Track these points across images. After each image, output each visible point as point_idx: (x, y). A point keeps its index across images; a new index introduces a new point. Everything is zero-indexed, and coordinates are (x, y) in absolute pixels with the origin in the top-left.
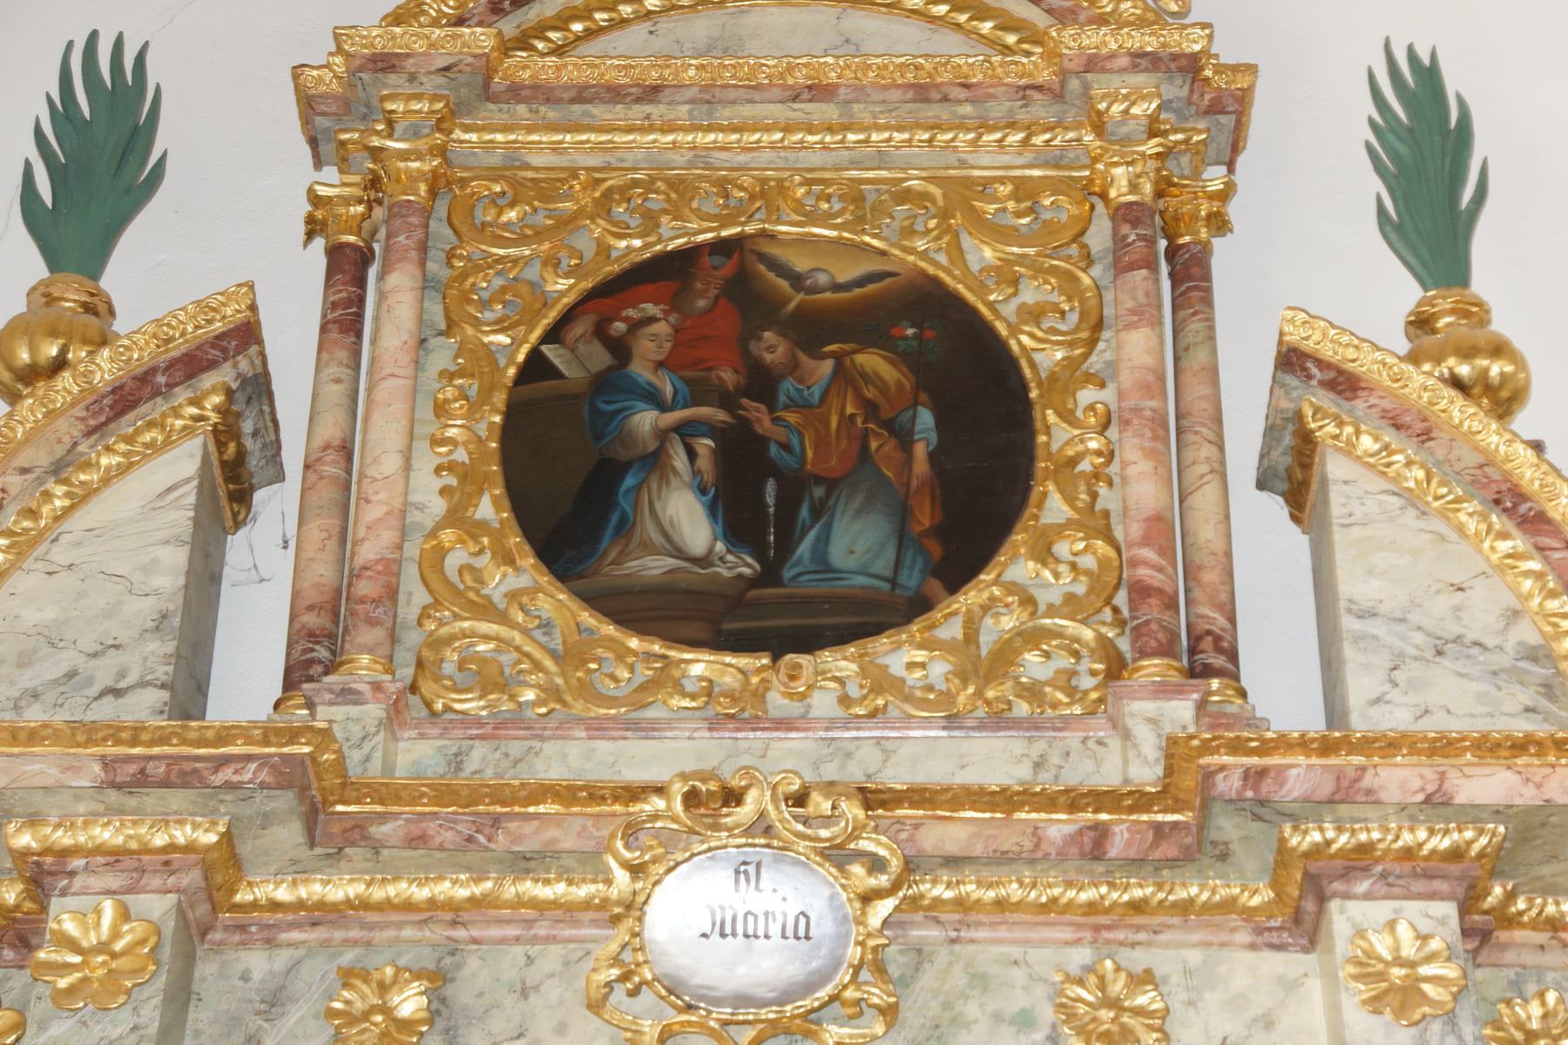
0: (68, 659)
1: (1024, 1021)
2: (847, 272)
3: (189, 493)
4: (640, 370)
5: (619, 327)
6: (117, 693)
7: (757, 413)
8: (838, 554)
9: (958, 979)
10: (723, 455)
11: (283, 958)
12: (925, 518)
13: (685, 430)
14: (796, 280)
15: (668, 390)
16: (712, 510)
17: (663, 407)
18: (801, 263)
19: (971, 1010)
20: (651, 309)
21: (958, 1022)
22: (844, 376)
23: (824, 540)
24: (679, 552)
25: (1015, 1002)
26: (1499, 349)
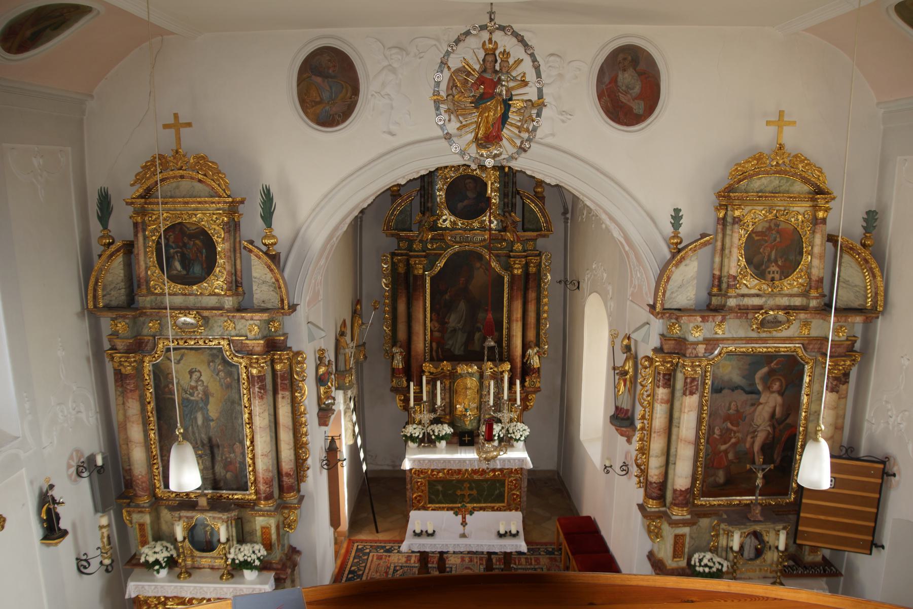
0: (114, 285)
1: (220, 326)
2: (194, 227)
3: (122, 263)
4: (171, 243)
5: (167, 236)
6: (120, 289)
7: (184, 249)
8: (195, 271)
9: (213, 321)
10: (181, 256)
11: (144, 318)
12: (205, 266)
13: (177, 252)
14: (188, 228)
15: (174, 246)
16: (180, 264)
17: (174, 249)
18: (188, 226)
19: (215, 325)
20: (171, 233)
21: (214, 327)
22: (195, 244)
23: (193, 269)
24: (177, 270)
25: (219, 324)
26: (274, 237)
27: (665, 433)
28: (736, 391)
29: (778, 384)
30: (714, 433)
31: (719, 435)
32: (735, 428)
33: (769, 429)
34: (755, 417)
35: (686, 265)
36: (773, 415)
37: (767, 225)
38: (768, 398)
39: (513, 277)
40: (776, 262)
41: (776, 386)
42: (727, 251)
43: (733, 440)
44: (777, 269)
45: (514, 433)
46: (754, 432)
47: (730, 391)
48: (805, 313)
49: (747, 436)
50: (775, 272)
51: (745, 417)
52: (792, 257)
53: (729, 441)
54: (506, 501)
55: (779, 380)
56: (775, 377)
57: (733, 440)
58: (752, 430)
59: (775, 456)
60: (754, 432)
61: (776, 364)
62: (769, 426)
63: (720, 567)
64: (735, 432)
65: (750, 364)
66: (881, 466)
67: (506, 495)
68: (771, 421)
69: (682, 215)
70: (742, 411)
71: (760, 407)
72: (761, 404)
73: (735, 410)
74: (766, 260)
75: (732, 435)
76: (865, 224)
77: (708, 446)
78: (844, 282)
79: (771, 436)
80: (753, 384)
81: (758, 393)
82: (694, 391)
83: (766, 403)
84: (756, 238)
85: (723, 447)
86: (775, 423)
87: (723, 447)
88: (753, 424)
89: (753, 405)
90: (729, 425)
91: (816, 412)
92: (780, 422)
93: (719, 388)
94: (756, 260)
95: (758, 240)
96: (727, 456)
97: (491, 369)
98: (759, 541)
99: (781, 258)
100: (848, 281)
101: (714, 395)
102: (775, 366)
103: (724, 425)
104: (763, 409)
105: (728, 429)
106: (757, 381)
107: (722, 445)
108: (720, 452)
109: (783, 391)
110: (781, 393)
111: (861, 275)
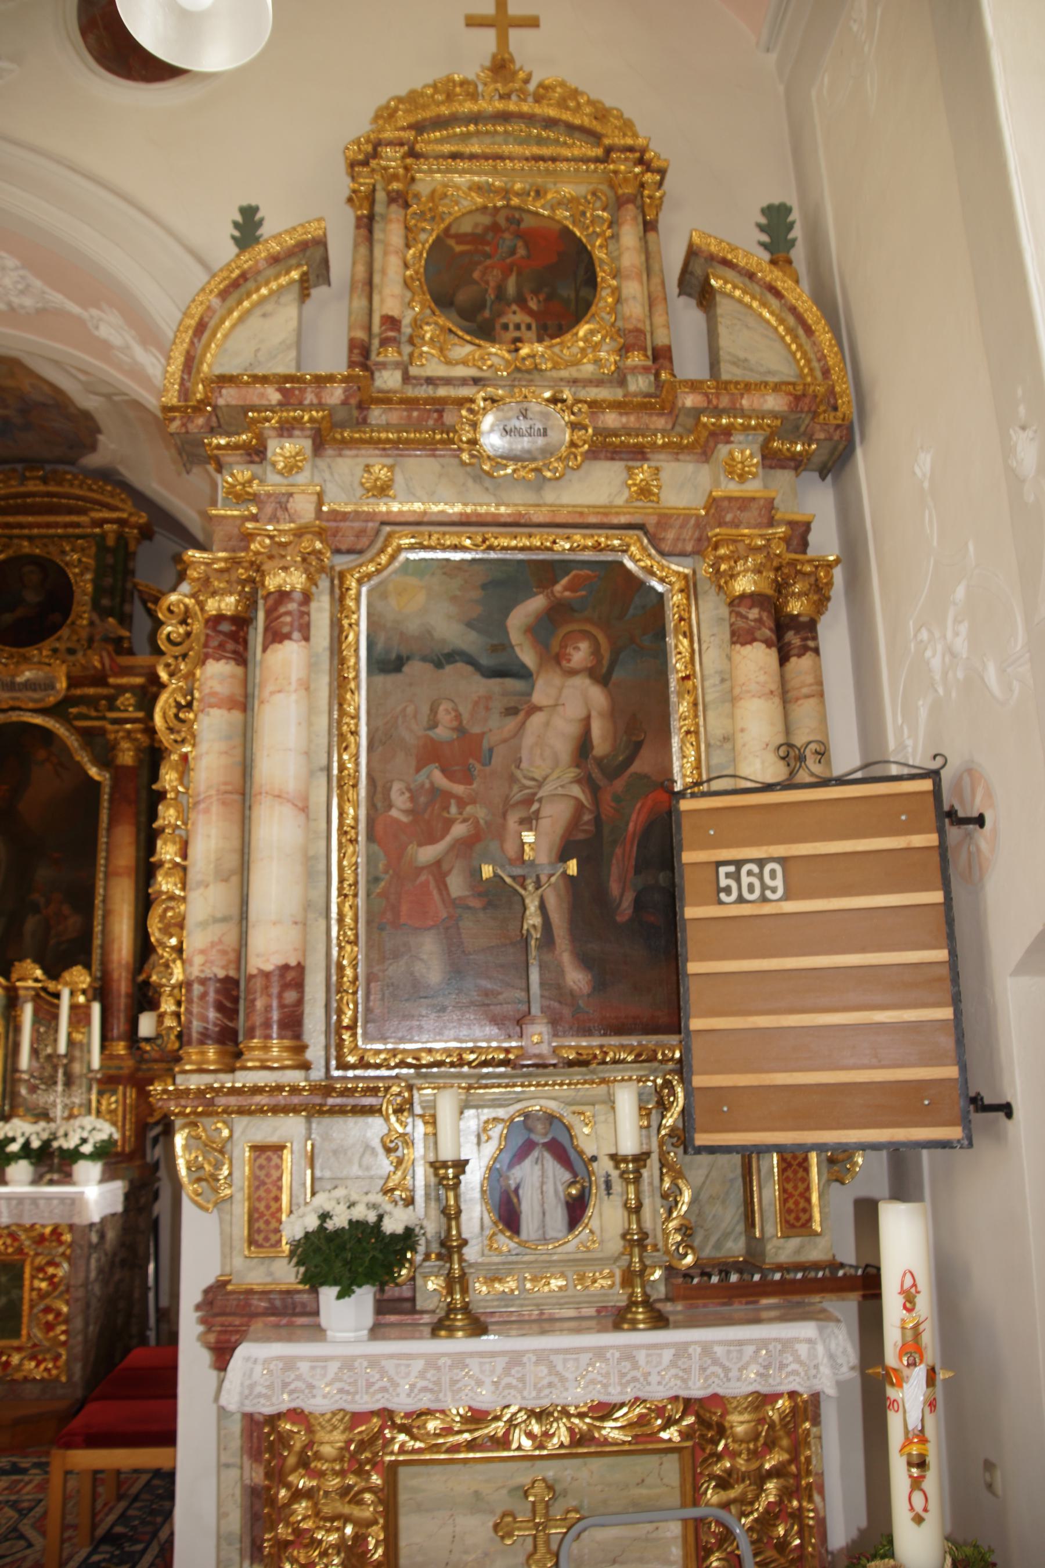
27: (224, 803)
28: (449, 669)
29: (584, 646)
30: (390, 806)
31: (406, 812)
32: (459, 789)
33: (576, 791)
34: (525, 755)
35: (264, 315)
36: (583, 746)
37: (486, 220)
38: (561, 690)
39: (119, 773)
40: (521, 301)
41: (580, 654)
42: (377, 279)
43: (459, 830)
44: (528, 319)
45: (66, 1135)
46: (529, 801)
47: (429, 667)
48: (621, 414)
49: (504, 815)
50: (523, 327)
51: (491, 750)
52: (566, 292)
53: (446, 830)
54: (24, 1332)
55: (586, 635)
56: (575, 627)
57: (459, 830)
58: (518, 797)
59: (615, 888)
60: (529, 801)
61: (570, 587)
62: (578, 781)
63: (372, 1218)
64: (462, 803)
65: (484, 587)
66: (927, 785)
67: (26, 1307)
68: (578, 766)
69: (261, 221)
70: (476, 730)
71: (537, 719)
72: (539, 709)
73: (453, 729)
74: (491, 296)
75: (453, 810)
76: (765, 238)
77: (375, 847)
78: (734, 364)
79: (587, 817)
80: (503, 646)
81: (522, 673)
82: (286, 630)
83: (556, 705)
84: (458, 248)
85: (427, 854)
86: (596, 774)
87: (427, 854)
88: (519, 774)
89: (511, 711)
90: (439, 778)
91: (726, 739)
92: (613, 769)
93: (393, 656)
94: (463, 297)
95: (463, 253)
96: (442, 885)
97: (36, 980)
98: (575, 1175)
99: (536, 292)
100: (746, 360)
101: (380, 679)
102: (567, 594)
103: (422, 777)
104: (547, 724)
105: (435, 792)
106: (516, 636)
107: (421, 845)
108: (420, 870)
109: (604, 670)
110: (601, 676)
111: (778, 345)
